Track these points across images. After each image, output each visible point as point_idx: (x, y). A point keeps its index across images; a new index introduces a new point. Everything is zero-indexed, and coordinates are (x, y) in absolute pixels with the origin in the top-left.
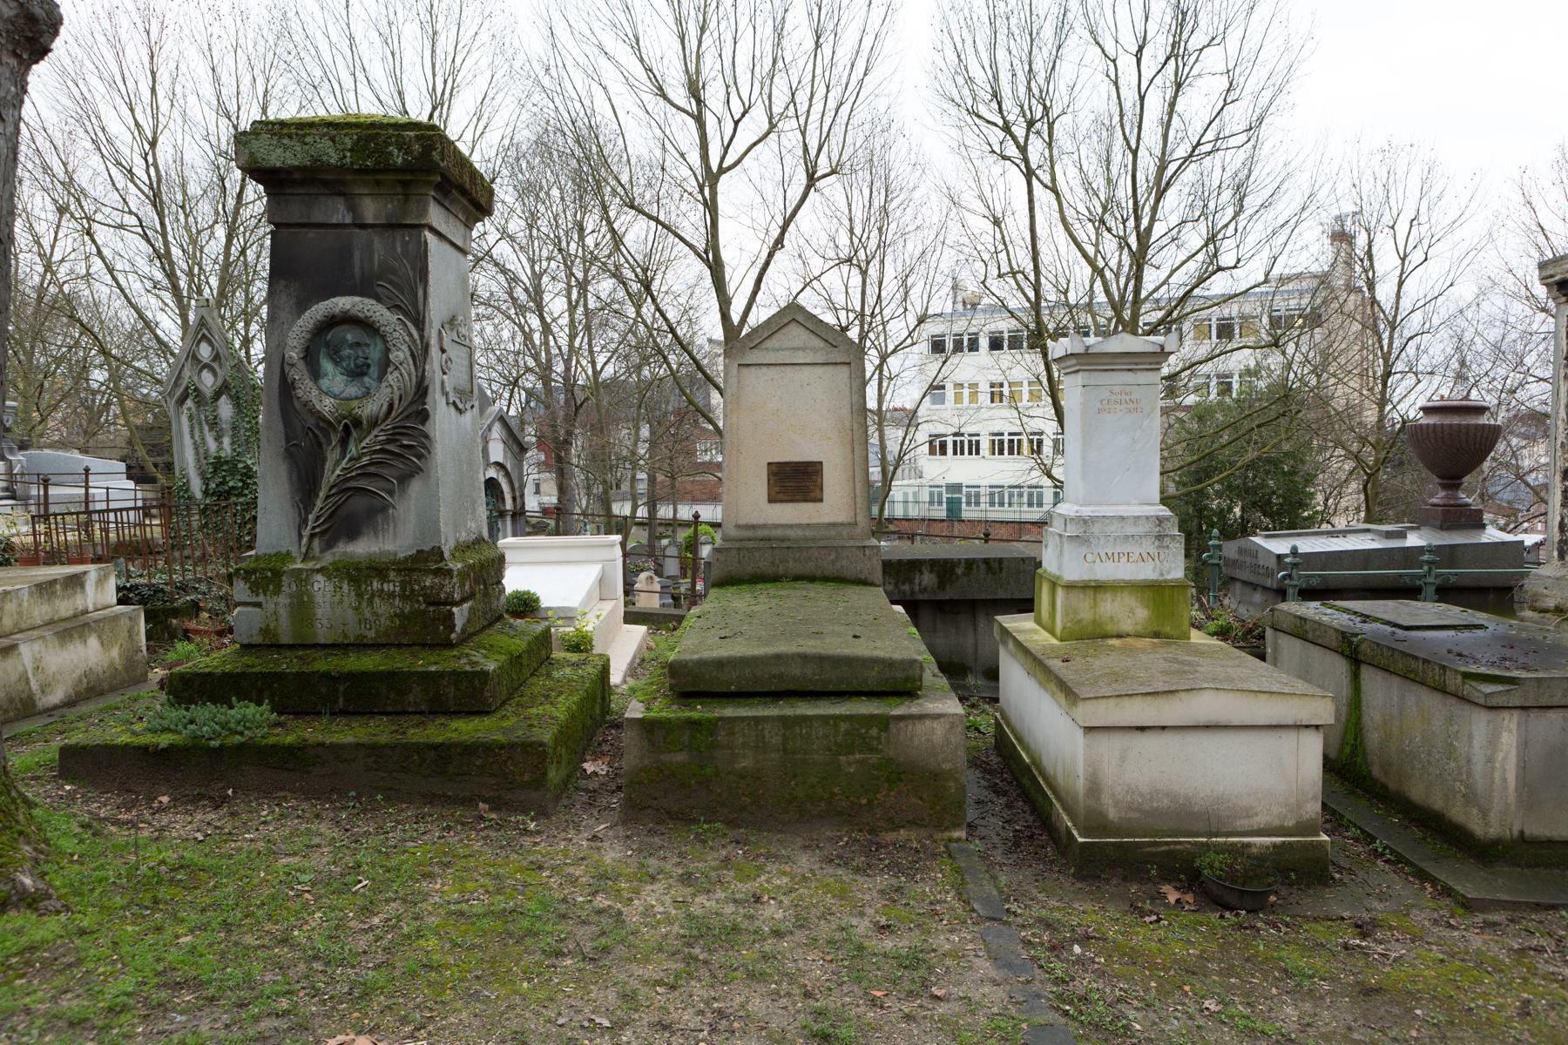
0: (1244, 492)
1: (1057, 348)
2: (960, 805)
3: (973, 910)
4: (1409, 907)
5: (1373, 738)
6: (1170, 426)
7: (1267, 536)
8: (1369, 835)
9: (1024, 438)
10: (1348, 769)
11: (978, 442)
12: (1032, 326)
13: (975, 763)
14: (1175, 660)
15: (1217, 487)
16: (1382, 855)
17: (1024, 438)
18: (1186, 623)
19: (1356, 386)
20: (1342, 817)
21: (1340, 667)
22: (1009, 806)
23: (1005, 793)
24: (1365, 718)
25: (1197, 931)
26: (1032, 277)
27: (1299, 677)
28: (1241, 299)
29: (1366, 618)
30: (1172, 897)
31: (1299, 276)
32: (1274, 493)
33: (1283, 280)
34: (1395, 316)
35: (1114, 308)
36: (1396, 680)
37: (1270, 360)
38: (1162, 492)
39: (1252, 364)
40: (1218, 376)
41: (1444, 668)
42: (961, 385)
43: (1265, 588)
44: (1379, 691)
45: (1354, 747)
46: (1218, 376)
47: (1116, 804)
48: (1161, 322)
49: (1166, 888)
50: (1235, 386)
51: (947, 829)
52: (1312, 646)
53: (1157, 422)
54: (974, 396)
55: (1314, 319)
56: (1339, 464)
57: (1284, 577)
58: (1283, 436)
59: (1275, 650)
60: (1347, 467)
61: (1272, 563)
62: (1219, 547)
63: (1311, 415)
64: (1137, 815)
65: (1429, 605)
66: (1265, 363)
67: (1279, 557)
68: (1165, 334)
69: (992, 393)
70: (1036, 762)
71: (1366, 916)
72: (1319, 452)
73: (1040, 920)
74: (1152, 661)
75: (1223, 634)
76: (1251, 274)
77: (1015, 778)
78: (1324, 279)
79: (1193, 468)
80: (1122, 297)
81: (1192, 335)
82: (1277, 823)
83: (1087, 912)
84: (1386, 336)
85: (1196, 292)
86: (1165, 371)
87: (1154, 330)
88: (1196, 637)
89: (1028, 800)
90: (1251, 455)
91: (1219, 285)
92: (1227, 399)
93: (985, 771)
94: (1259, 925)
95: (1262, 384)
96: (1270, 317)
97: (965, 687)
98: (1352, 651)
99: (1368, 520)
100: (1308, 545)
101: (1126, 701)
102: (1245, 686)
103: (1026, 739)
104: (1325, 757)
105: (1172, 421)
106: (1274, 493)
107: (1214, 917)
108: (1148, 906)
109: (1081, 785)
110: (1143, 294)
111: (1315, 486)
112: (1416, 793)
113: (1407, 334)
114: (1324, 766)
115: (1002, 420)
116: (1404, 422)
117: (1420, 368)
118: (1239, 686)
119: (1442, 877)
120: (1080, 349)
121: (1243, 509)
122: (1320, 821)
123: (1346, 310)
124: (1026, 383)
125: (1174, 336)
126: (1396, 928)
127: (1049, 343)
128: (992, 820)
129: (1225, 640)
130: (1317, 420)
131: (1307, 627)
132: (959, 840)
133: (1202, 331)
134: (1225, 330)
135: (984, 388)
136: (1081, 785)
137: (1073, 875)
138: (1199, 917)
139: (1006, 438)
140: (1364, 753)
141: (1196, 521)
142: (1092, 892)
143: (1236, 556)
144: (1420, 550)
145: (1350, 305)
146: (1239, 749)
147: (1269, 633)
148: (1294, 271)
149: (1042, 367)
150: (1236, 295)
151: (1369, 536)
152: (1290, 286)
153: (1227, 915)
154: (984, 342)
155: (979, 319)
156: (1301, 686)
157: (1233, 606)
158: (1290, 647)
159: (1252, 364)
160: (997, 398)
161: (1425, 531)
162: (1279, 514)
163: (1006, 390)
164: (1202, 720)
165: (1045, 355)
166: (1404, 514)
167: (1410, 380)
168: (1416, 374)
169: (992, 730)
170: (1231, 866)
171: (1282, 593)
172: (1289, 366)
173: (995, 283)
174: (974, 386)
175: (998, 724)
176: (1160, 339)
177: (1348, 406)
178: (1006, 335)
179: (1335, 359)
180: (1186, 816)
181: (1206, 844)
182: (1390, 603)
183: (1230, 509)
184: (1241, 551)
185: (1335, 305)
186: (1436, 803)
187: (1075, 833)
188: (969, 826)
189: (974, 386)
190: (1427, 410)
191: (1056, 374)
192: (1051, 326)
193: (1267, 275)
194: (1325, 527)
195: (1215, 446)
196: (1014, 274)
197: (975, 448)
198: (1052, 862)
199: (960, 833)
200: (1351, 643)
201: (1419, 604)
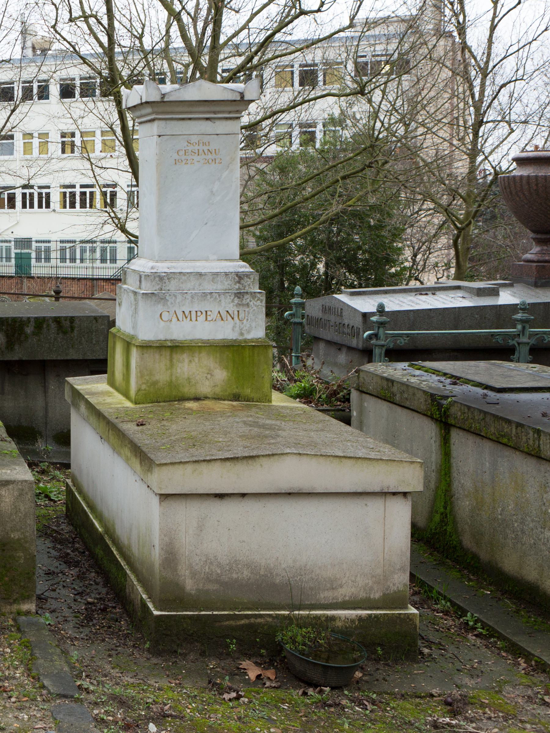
0: (328, 247)
1: (132, 96)
2: (30, 576)
3: (43, 687)
4: (501, 684)
5: (464, 506)
6: (250, 178)
7: (352, 294)
8: (460, 608)
9: (97, 190)
10: (439, 539)
11: (48, 195)
12: (105, 73)
13: (45, 532)
14: (256, 424)
15: (300, 242)
16: (474, 628)
17: (97, 190)
18: (267, 385)
19: (447, 136)
20: (431, 589)
21: (429, 431)
22: (81, 577)
23: (77, 564)
24: (455, 485)
25: (278, 708)
26: (105, 22)
27: (386, 442)
28: (325, 44)
29: (456, 380)
30: (252, 674)
31: (386, 20)
32: (359, 248)
33: (369, 24)
34: (487, 63)
35: (191, 54)
36: (488, 446)
37: (355, 109)
38: (242, 247)
39: (337, 113)
40: (301, 125)
41: (538, 432)
42: (31, 135)
43: (350, 349)
44: (471, 457)
45: (444, 515)
46: (301, 125)
47: (194, 575)
48: (241, 68)
49: (246, 664)
50: (319, 136)
51: (15, 601)
52: (399, 409)
53: (237, 174)
54: (44, 146)
55: (402, 66)
56: (429, 218)
57: (370, 337)
58: (369, 188)
59: (361, 413)
60: (436, 221)
61: (358, 322)
62: (302, 305)
63: (399, 167)
64: (215, 587)
65: (523, 366)
66: (350, 112)
67: (365, 316)
68: (245, 81)
69: (63, 143)
70: (110, 531)
71: (457, 693)
72: (407, 206)
73: (114, 697)
74: (231, 425)
75: (306, 396)
76: (336, 17)
77: (87, 548)
78: (412, 24)
79: (274, 222)
80: (200, 42)
81: (273, 82)
82: (362, 595)
83: (165, 689)
84: (477, 83)
85: (278, 37)
86: (245, 120)
87: (233, 77)
88: (278, 400)
89: (102, 571)
90: (335, 208)
91: (301, 29)
92: (311, 150)
93: (55, 540)
94: (344, 702)
95: (347, 134)
96: (356, 63)
97: (35, 453)
98: (442, 415)
99: (459, 276)
100: (395, 303)
101: (204, 467)
102: (330, 452)
103: (100, 506)
104: (414, 526)
105: (252, 173)
106: (359, 248)
107: (296, 694)
108: (227, 682)
109: (156, 555)
110: (222, 39)
111: (403, 241)
112: (509, 564)
113: (499, 81)
114: (412, 535)
115: (73, 172)
116: (496, 174)
117: (514, 117)
118: (324, 451)
119: (537, 652)
120: (156, 97)
121: (327, 265)
122: (408, 592)
123: (435, 55)
124: (98, 133)
125: (254, 83)
126: (488, 706)
127: (124, 90)
128: (64, 592)
129: (308, 403)
130: (405, 172)
131: (395, 389)
132: (28, 613)
133: (284, 78)
134: (308, 77)
135: (55, 137)
136: (156, 555)
137: (148, 650)
138: (281, 693)
139: (78, 190)
140: (455, 522)
141: (277, 277)
142: (168, 668)
143: (319, 315)
144: (513, 308)
145: (440, 51)
146: (325, 517)
147: (354, 395)
148: (381, 15)
149: (116, 116)
150: (320, 40)
151: (460, 293)
152: (377, 31)
153: (311, 692)
154: (54, 90)
155: (49, 66)
156: (387, 451)
157: (317, 367)
158: (376, 410)
159: (337, 113)
160: (68, 149)
161: (519, 288)
162: (365, 270)
163: (77, 140)
164: (284, 487)
165: (119, 103)
166: (497, 270)
167: (503, 129)
168: (509, 123)
169: (62, 497)
170: (314, 641)
171: (367, 354)
172: (375, 115)
173: (67, 27)
174: (44, 136)
175: (69, 491)
176: (239, 86)
177: (438, 157)
178: (78, 83)
179: (424, 108)
180: (267, 587)
181: (288, 618)
182: (482, 364)
183: (314, 265)
184: (326, 309)
185: (424, 51)
186: (531, 574)
187: (150, 605)
188: (39, 598)
189: (44, 136)
190: (521, 161)
191: (130, 124)
192: (125, 73)
193: (352, 19)
194: (413, 284)
195: (298, 199)
196: (86, 18)
197: (45, 201)
198: (126, 636)
199: (30, 606)
200: (440, 406)
201: (512, 365)
